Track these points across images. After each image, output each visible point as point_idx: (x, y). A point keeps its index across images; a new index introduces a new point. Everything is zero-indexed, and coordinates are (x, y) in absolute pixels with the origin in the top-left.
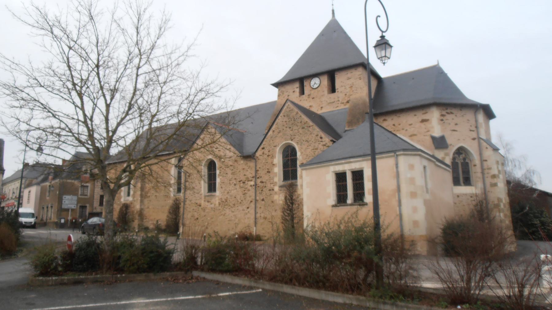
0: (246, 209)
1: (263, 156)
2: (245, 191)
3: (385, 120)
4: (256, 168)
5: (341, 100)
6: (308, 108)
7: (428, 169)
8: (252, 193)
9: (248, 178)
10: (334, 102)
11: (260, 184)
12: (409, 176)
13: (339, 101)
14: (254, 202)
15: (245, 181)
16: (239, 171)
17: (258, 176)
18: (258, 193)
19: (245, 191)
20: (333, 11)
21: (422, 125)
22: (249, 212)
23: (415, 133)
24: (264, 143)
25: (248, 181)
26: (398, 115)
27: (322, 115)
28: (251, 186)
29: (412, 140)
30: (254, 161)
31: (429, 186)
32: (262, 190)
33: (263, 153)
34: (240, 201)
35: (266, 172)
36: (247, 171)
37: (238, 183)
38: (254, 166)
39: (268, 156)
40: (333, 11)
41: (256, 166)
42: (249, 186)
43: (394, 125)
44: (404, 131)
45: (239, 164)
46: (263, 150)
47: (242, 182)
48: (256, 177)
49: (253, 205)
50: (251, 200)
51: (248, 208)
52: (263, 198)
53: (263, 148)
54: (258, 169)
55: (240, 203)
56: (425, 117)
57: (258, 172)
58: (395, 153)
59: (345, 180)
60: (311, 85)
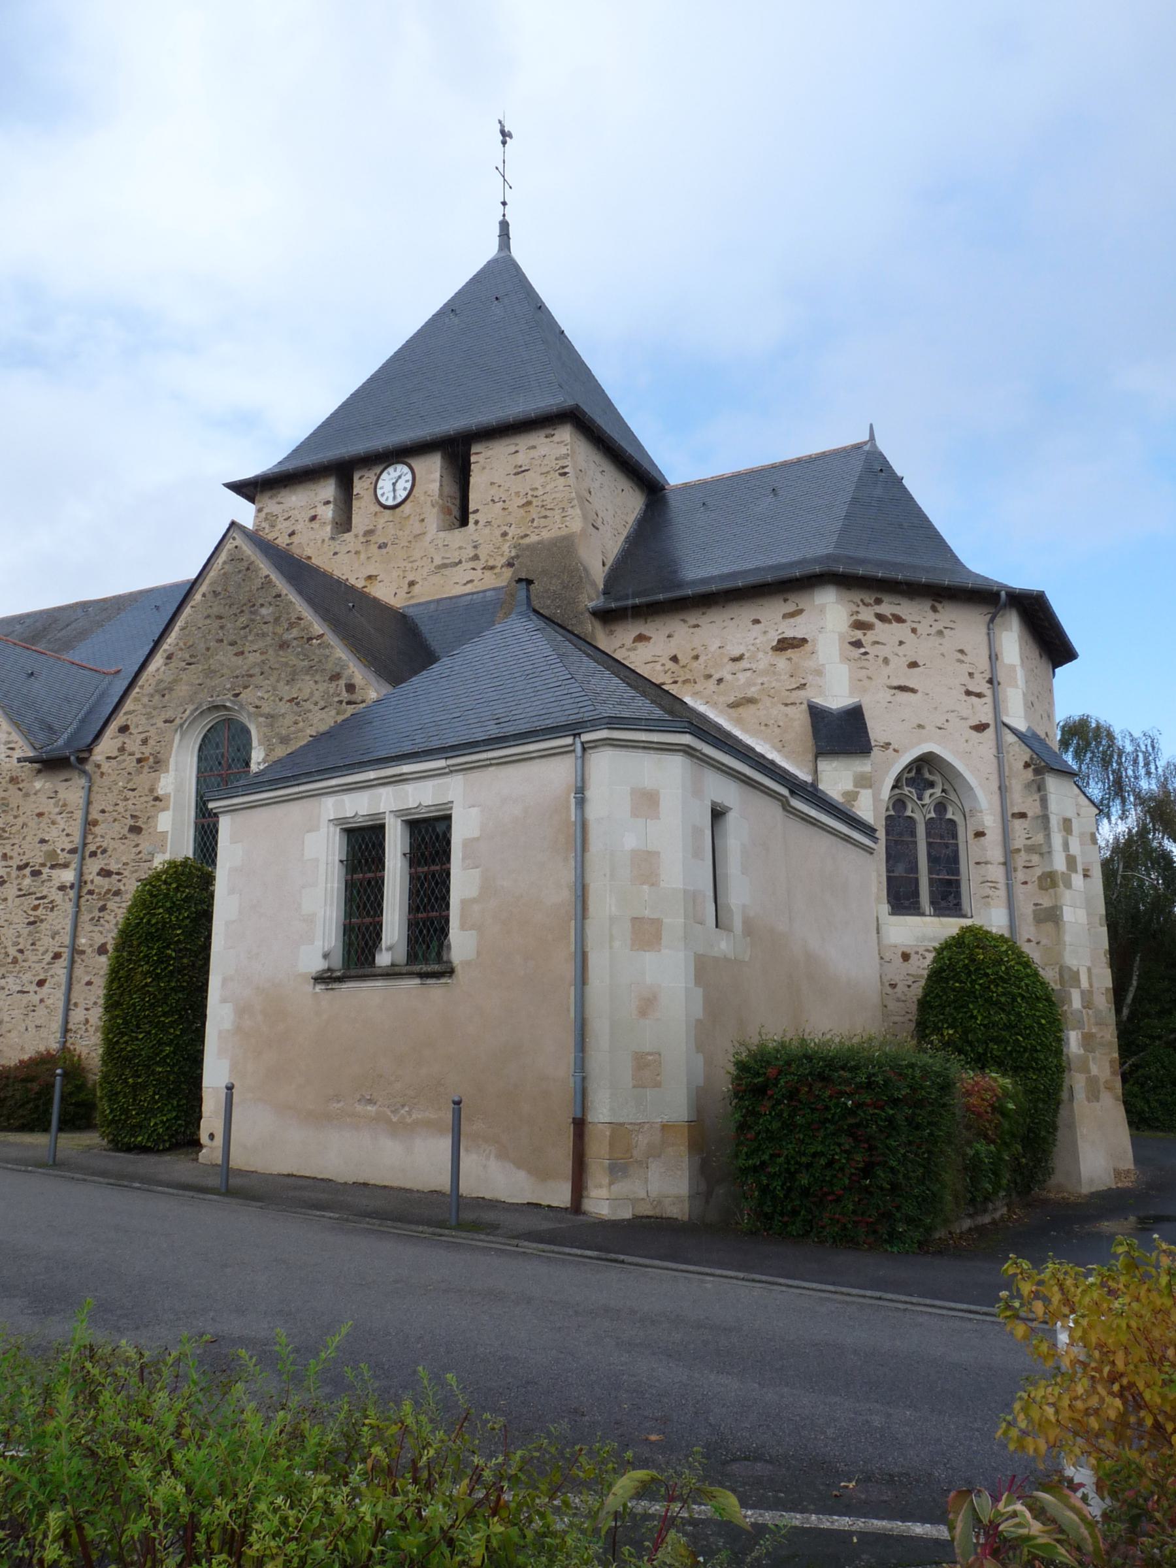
0: (34, 987)
1: (119, 763)
2: (35, 908)
3: (641, 638)
4: (87, 813)
5: (483, 557)
6: (359, 584)
7: (736, 827)
8: (61, 920)
9: (52, 854)
10: (460, 562)
11: (99, 880)
12: (630, 842)
13: (476, 558)
14: (63, 962)
15: (43, 865)
16: (24, 825)
17: (92, 848)
18: (85, 917)
19: (35, 908)
20: (504, 226)
21: (781, 662)
22: (42, 1001)
23: (752, 692)
24: (129, 705)
25: (53, 867)
26: (693, 618)
27: (410, 612)
28: (62, 888)
29: (739, 721)
30: (83, 781)
31: (738, 895)
32: (103, 909)
33: (122, 749)
34: (12, 951)
35: (125, 831)
36: (53, 823)
37: (14, 873)
38: (82, 802)
39: (139, 761)
40: (504, 226)
41: (89, 803)
42: (54, 890)
43: (674, 659)
44: (711, 685)
45: (27, 795)
46: (122, 738)
47: (27, 871)
48: (82, 852)
49: (60, 970)
50: (57, 950)
51: (41, 983)
52: (103, 941)
53: (124, 729)
54: (95, 815)
55: (15, 961)
56: (792, 629)
57: (97, 830)
58: (575, 735)
59: (379, 862)
60: (379, 492)
